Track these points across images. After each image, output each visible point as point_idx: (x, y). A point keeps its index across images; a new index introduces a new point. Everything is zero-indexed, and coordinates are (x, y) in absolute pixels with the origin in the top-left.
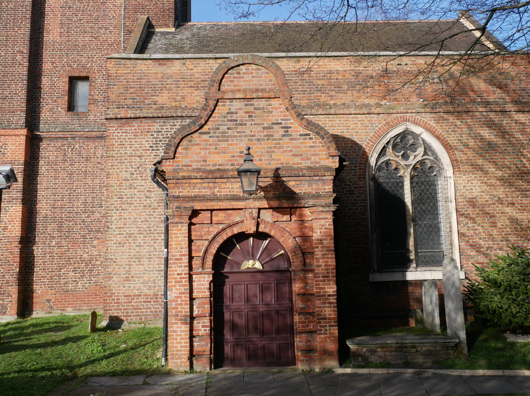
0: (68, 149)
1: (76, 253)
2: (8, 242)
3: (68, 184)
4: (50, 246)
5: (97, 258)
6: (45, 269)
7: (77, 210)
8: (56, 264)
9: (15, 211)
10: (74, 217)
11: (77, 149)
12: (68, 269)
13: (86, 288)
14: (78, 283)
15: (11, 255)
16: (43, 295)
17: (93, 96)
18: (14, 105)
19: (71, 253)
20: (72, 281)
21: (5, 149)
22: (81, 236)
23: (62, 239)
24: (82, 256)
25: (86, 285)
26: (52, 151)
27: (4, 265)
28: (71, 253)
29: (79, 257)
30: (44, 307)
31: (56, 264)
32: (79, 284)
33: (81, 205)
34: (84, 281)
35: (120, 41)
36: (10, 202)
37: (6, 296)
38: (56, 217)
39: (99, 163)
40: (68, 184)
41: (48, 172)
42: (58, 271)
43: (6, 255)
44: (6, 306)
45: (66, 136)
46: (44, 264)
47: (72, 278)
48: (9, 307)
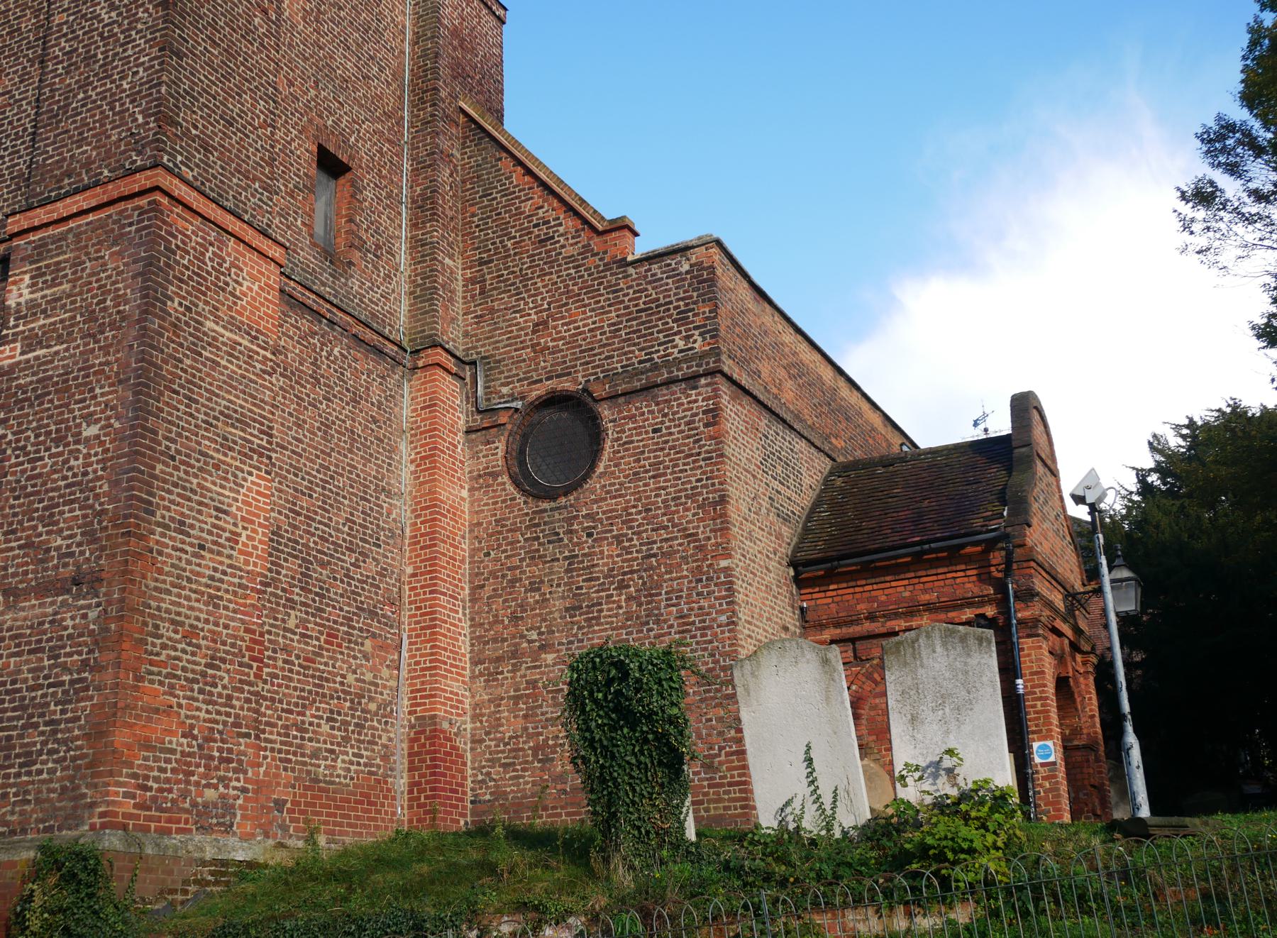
0: (322, 350)
1: (334, 667)
2: (240, 586)
3: (322, 452)
4: (285, 629)
5: (370, 691)
6: (273, 700)
7: (338, 538)
8: (295, 689)
9: (258, 493)
10: (332, 556)
11: (336, 358)
12: (318, 709)
13: (352, 779)
14: (334, 760)
15: (247, 630)
16: (270, 782)
17: (357, 225)
18: (248, 157)
19: (326, 664)
20: (327, 750)
21: (237, 282)
22: (344, 617)
23: (307, 613)
24: (344, 676)
25: (353, 768)
26: (292, 338)
27: (232, 663)
28: (326, 664)
29: (338, 679)
30: (271, 823)
31: (295, 689)
32: (339, 764)
33: (344, 525)
34: (347, 753)
35: (403, 118)
36: (245, 455)
37: (236, 771)
38: (297, 543)
39: (375, 421)
40: (322, 452)
41: (284, 398)
42: (299, 714)
43: (235, 629)
44: (233, 806)
45: (323, 311)
46: (273, 685)
47: (325, 742)
48: (241, 807)
